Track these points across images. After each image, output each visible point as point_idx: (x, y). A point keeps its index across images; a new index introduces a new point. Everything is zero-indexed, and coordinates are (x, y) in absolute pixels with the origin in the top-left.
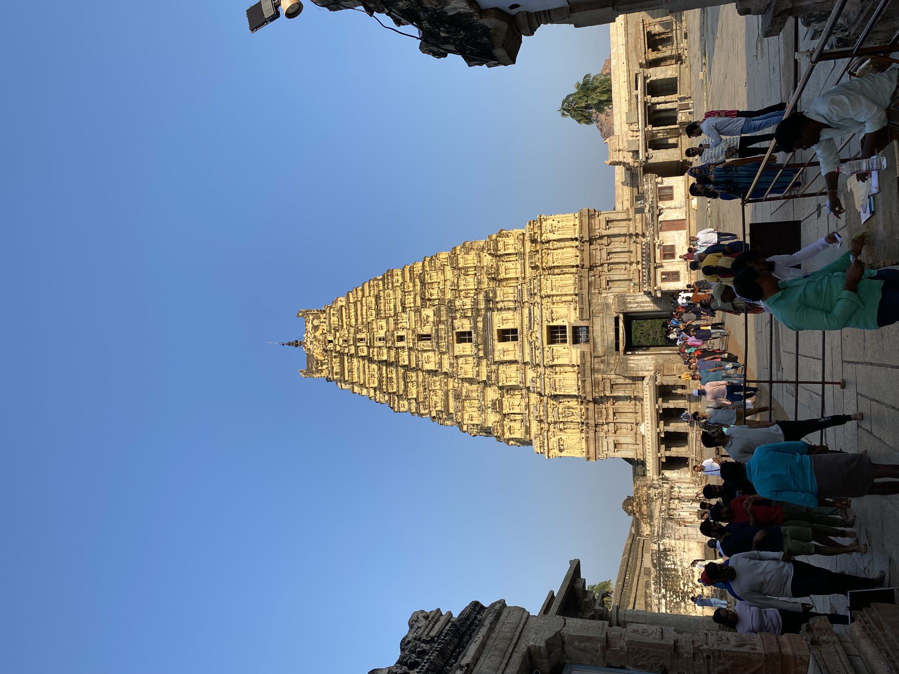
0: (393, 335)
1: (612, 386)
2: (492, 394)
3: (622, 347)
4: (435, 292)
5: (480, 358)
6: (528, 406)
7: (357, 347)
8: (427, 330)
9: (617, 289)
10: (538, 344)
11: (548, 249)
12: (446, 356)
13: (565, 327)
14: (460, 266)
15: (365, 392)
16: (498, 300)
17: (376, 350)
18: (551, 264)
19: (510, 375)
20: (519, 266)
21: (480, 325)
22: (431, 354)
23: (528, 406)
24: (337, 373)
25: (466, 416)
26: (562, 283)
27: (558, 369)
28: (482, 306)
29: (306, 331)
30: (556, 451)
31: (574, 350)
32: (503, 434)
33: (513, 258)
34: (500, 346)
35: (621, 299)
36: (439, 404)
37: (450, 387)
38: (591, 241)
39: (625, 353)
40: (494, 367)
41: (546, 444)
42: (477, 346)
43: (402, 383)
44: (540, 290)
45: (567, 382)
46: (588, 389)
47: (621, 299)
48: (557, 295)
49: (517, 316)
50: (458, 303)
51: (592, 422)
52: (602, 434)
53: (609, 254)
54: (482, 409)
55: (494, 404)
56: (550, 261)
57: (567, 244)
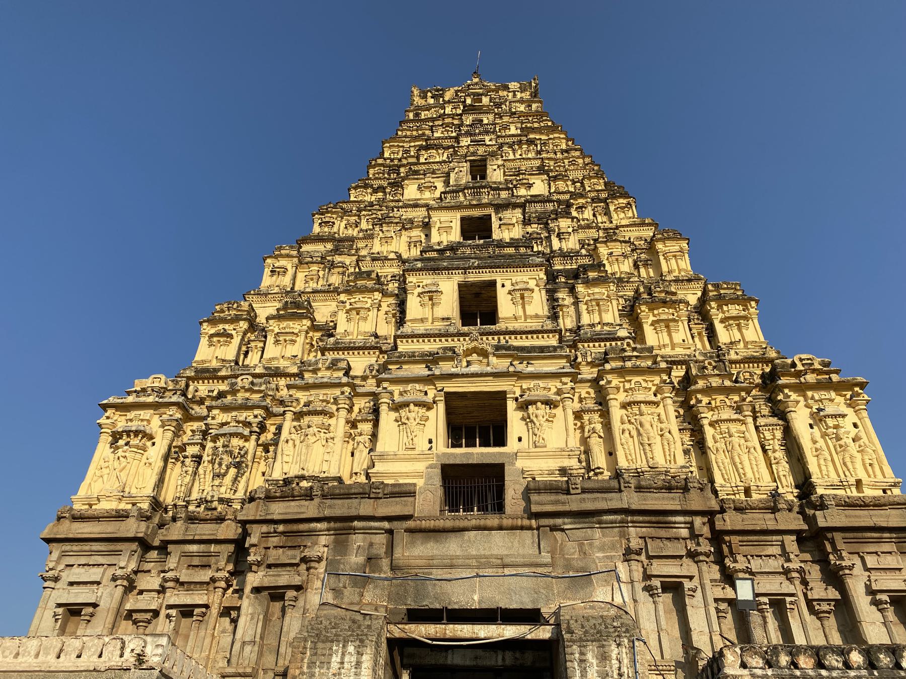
0: (487, 132)
1: (276, 594)
3: (423, 631)
4: (588, 214)
6: (278, 373)
9: (653, 617)
10: (446, 367)
11: (754, 411)
13: (501, 441)
14: (660, 246)
16: (580, 288)
17: (456, 122)
18: (707, 417)
20: (679, 351)
24: (417, 115)
25: (283, 262)
26: (654, 433)
27: (366, 427)
30: (121, 425)
31: (421, 466)
32: (213, 322)
33: (701, 345)
34: (449, 287)
35: (619, 628)
36: (326, 229)
37: (361, 244)
38: (814, 540)
39: (393, 644)
40: (393, 287)
41: (142, 399)
42: (453, 248)
44: (621, 372)
45: (318, 450)
46: (278, 510)
47: (619, 628)
48: (607, 426)
50: (564, 224)
51: (176, 531)
52: (127, 562)
53: (778, 604)
55: (298, 305)
56: (715, 412)
57: (783, 468)
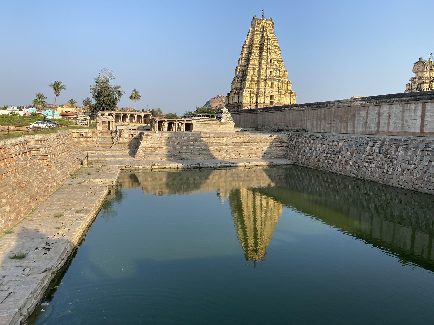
2: (256, 79)
5: (266, 77)
6: (254, 88)
7: (267, 39)
8: (272, 62)
12: (265, 67)
15: (249, 37)
19: (262, 84)
21: (274, 78)
22: (266, 62)
23: (254, 88)
28: (278, 79)
29: (266, 20)
43: (256, 51)
49: (276, 88)
54: (252, 75)
55: (254, 79)
